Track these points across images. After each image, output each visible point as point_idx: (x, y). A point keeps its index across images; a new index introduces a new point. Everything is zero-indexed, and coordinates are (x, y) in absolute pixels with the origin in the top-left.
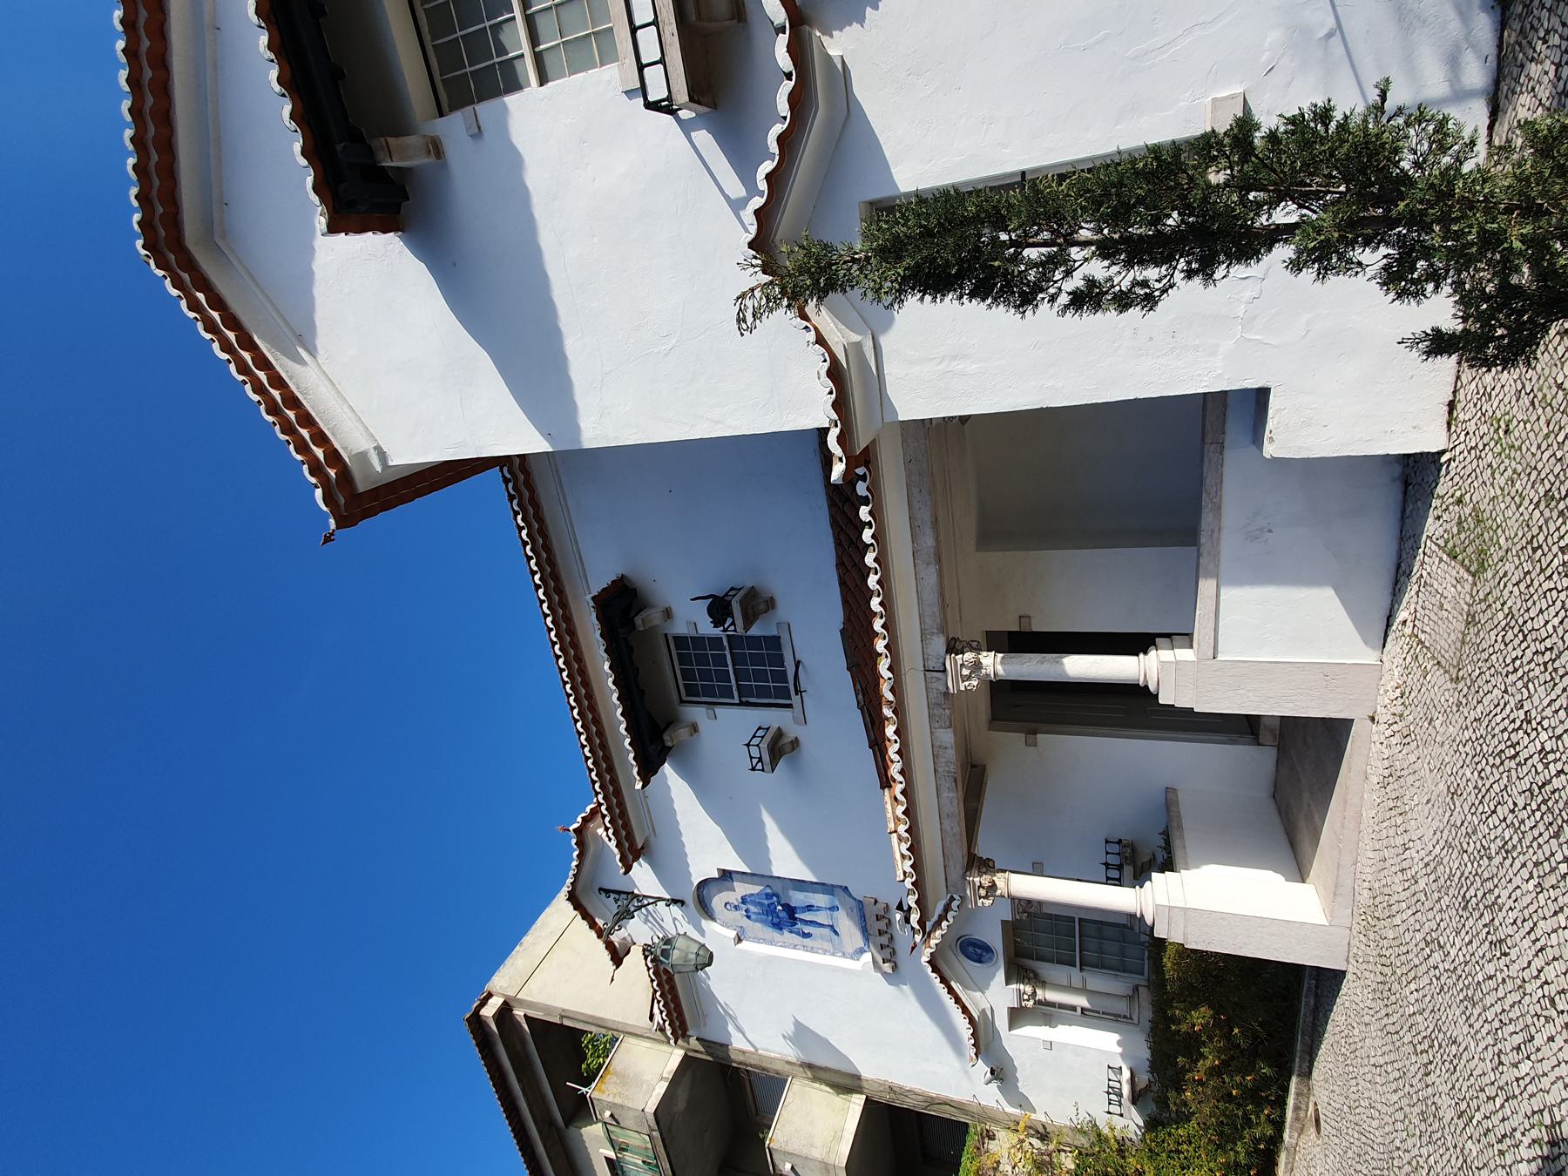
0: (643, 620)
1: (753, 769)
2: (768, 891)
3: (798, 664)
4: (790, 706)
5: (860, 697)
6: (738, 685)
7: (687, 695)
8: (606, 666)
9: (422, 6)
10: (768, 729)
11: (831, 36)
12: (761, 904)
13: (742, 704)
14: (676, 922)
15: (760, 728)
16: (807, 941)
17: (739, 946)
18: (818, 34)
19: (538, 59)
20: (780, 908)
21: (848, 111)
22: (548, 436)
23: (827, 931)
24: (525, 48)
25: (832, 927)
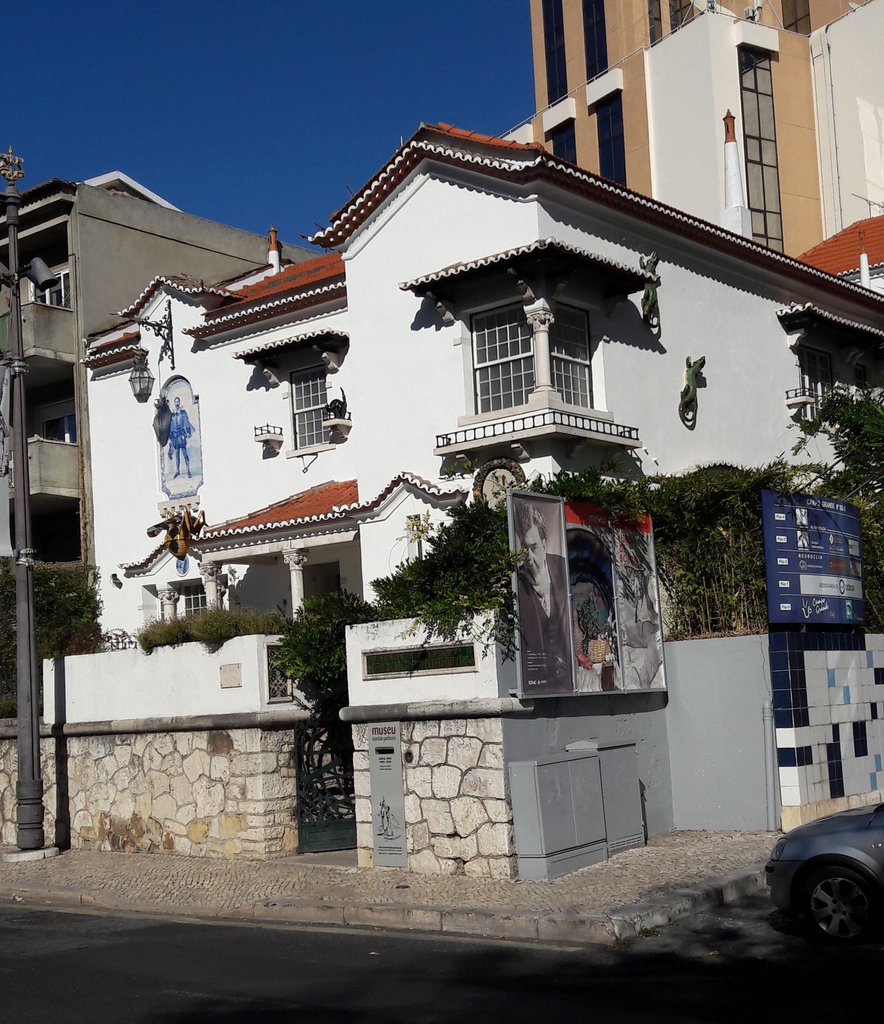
4: (296, 449)
5: (295, 497)
12: (183, 425)
13: (294, 415)
15: (281, 429)
16: (166, 456)
23: (176, 471)
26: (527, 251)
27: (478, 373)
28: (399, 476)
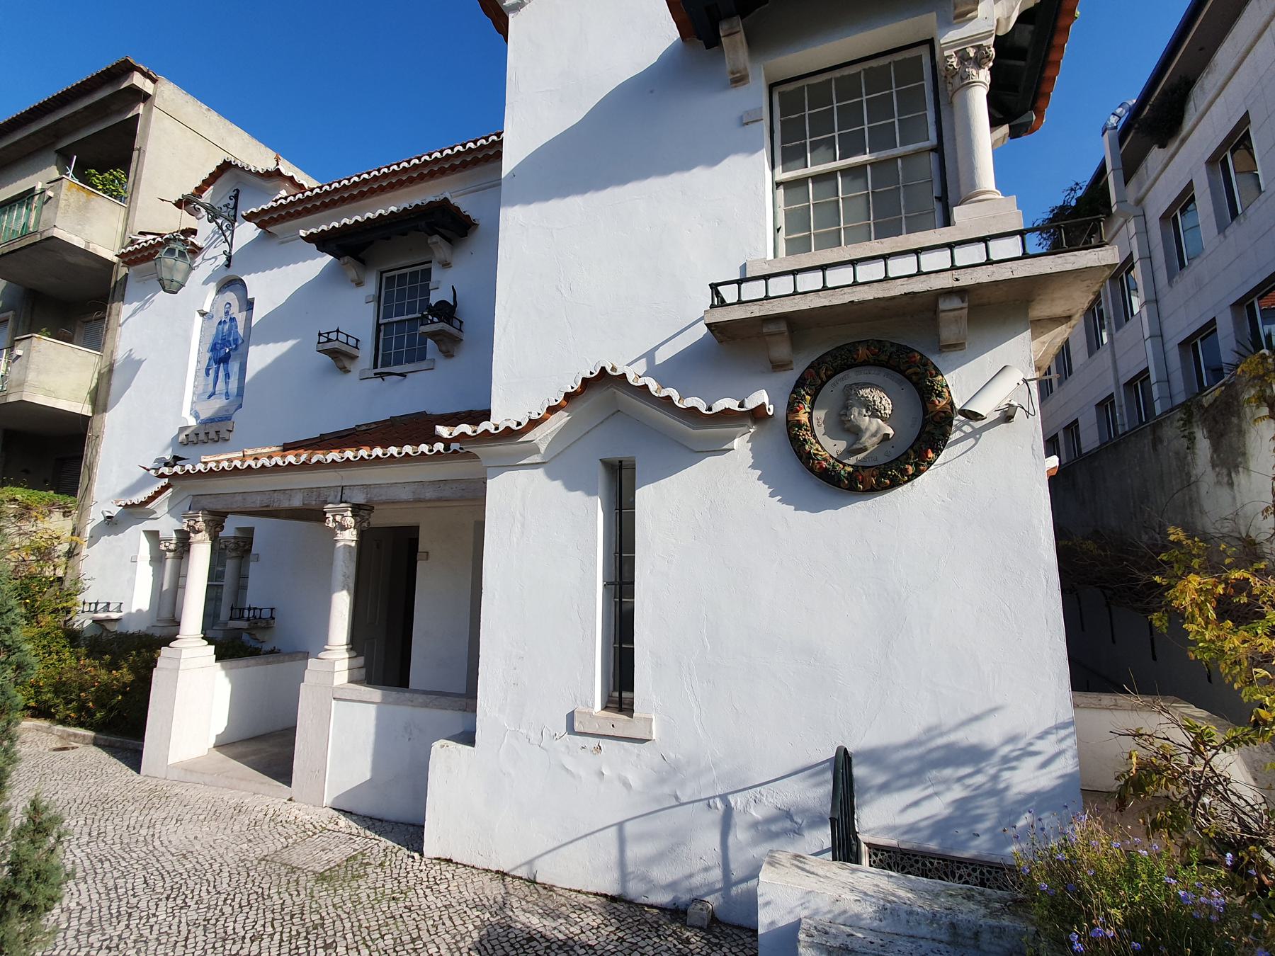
0: (436, 243)
1: (320, 335)
2: (240, 341)
3: (403, 375)
4: (375, 366)
5: (364, 428)
6: (393, 322)
7: (387, 278)
8: (394, 209)
9: (864, 70)
10: (357, 348)
11: (748, 442)
12: (230, 334)
13: (379, 326)
14: (214, 260)
15: (357, 340)
17: (197, 314)
18: (752, 431)
19: (801, 182)
20: (227, 350)
21: (696, 453)
22: (513, 174)
23: (211, 389)
24: (812, 170)
25: (213, 394)
28: (603, 369)
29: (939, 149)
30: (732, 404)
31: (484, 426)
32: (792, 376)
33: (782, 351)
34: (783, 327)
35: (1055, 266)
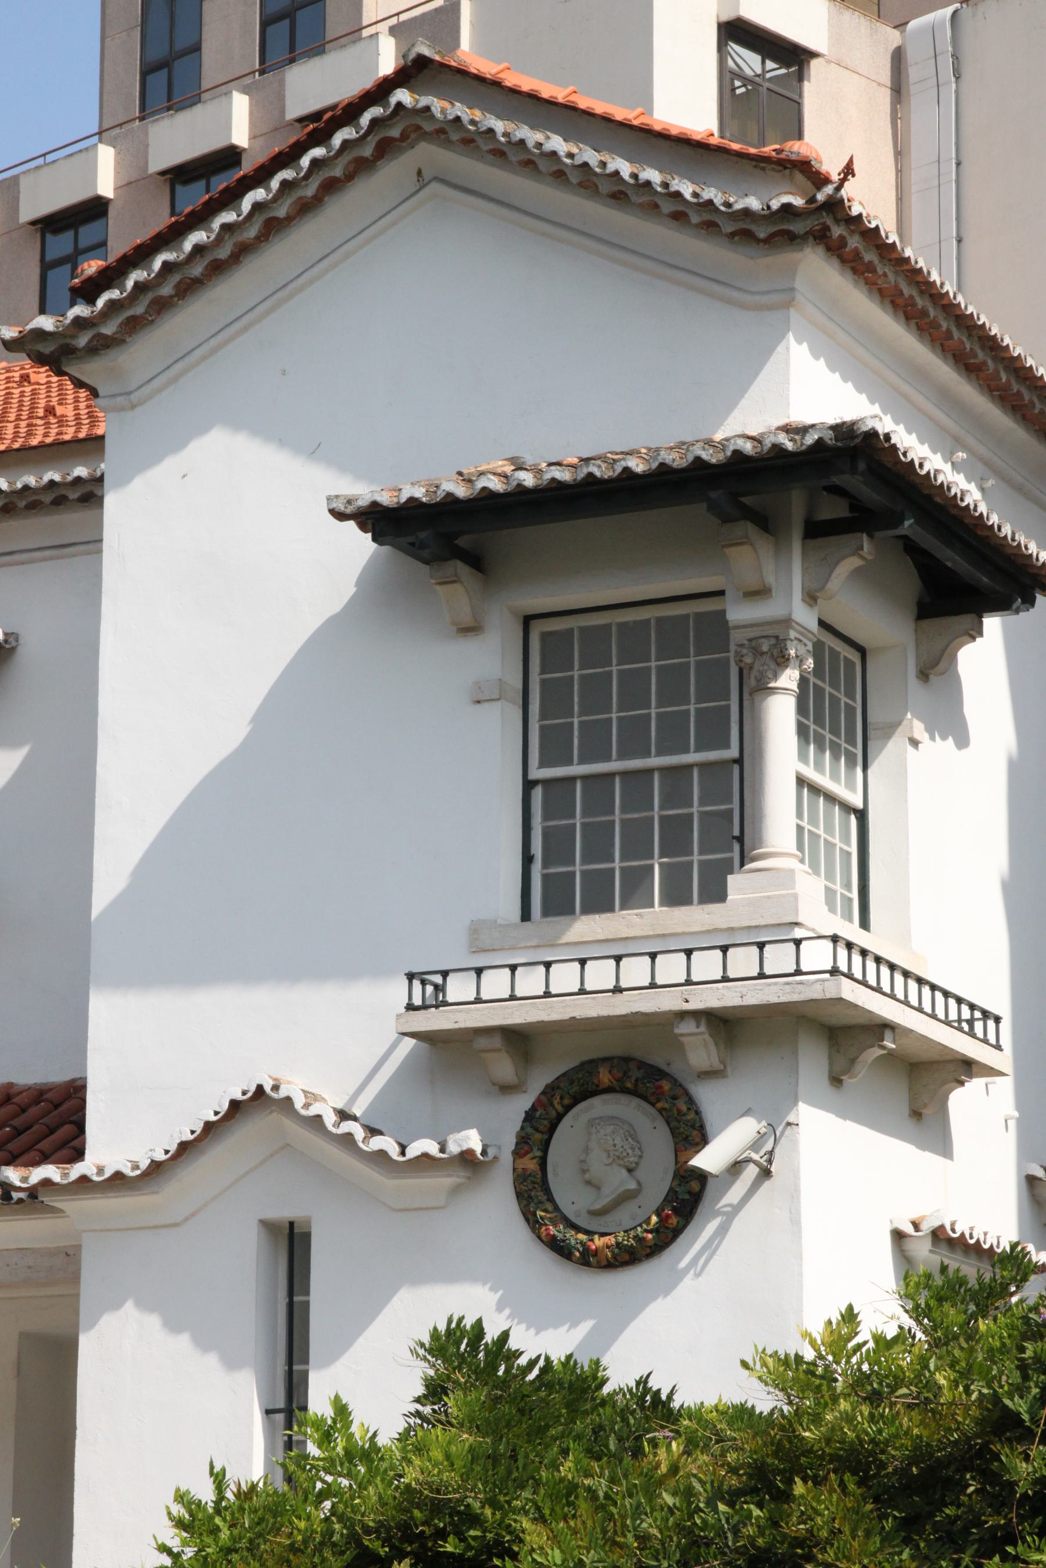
26: (790, 446)
27: (538, 793)
28: (260, 1089)
29: (739, 761)
30: (431, 1147)
31: (77, 1170)
32: (524, 1102)
33: (504, 1068)
34: (497, 1041)
35: (784, 994)
